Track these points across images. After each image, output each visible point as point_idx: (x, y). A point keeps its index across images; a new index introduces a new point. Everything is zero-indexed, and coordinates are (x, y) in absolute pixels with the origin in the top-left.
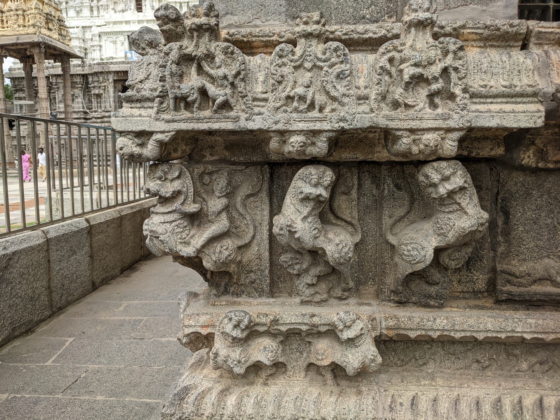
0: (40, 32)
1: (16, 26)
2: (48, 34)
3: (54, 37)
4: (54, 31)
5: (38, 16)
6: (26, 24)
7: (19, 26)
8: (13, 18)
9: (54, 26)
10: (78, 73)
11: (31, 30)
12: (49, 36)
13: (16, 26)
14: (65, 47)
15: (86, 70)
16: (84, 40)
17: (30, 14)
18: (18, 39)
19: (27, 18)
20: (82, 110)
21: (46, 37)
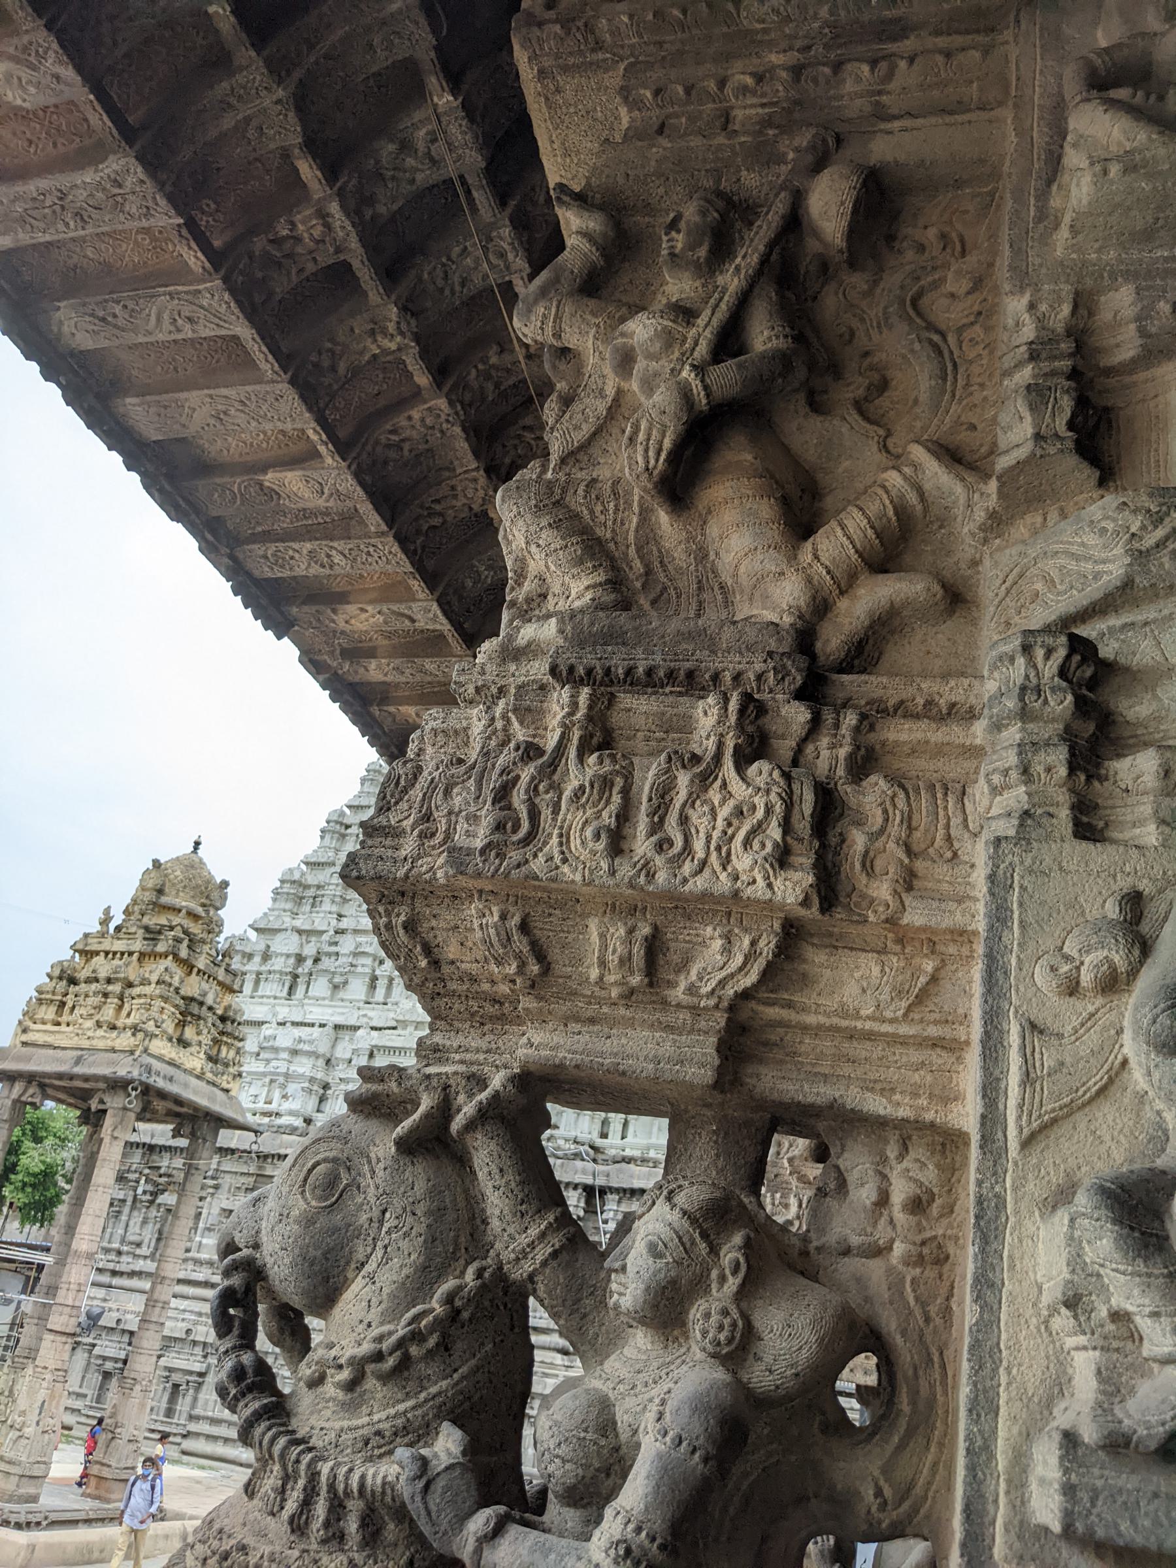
0: (146, 1050)
1: (89, 1024)
2: (173, 1055)
3: (188, 1066)
4: (194, 1049)
5: (158, 1003)
6: (119, 1024)
7: (99, 1025)
8: (90, 1001)
9: (198, 1034)
11: (125, 1040)
12: (171, 1063)
13: (89, 1024)
14: (212, 1099)
16: (328, 1062)
17: (139, 996)
18: (78, 1060)
19: (127, 1006)
21: (157, 1065)
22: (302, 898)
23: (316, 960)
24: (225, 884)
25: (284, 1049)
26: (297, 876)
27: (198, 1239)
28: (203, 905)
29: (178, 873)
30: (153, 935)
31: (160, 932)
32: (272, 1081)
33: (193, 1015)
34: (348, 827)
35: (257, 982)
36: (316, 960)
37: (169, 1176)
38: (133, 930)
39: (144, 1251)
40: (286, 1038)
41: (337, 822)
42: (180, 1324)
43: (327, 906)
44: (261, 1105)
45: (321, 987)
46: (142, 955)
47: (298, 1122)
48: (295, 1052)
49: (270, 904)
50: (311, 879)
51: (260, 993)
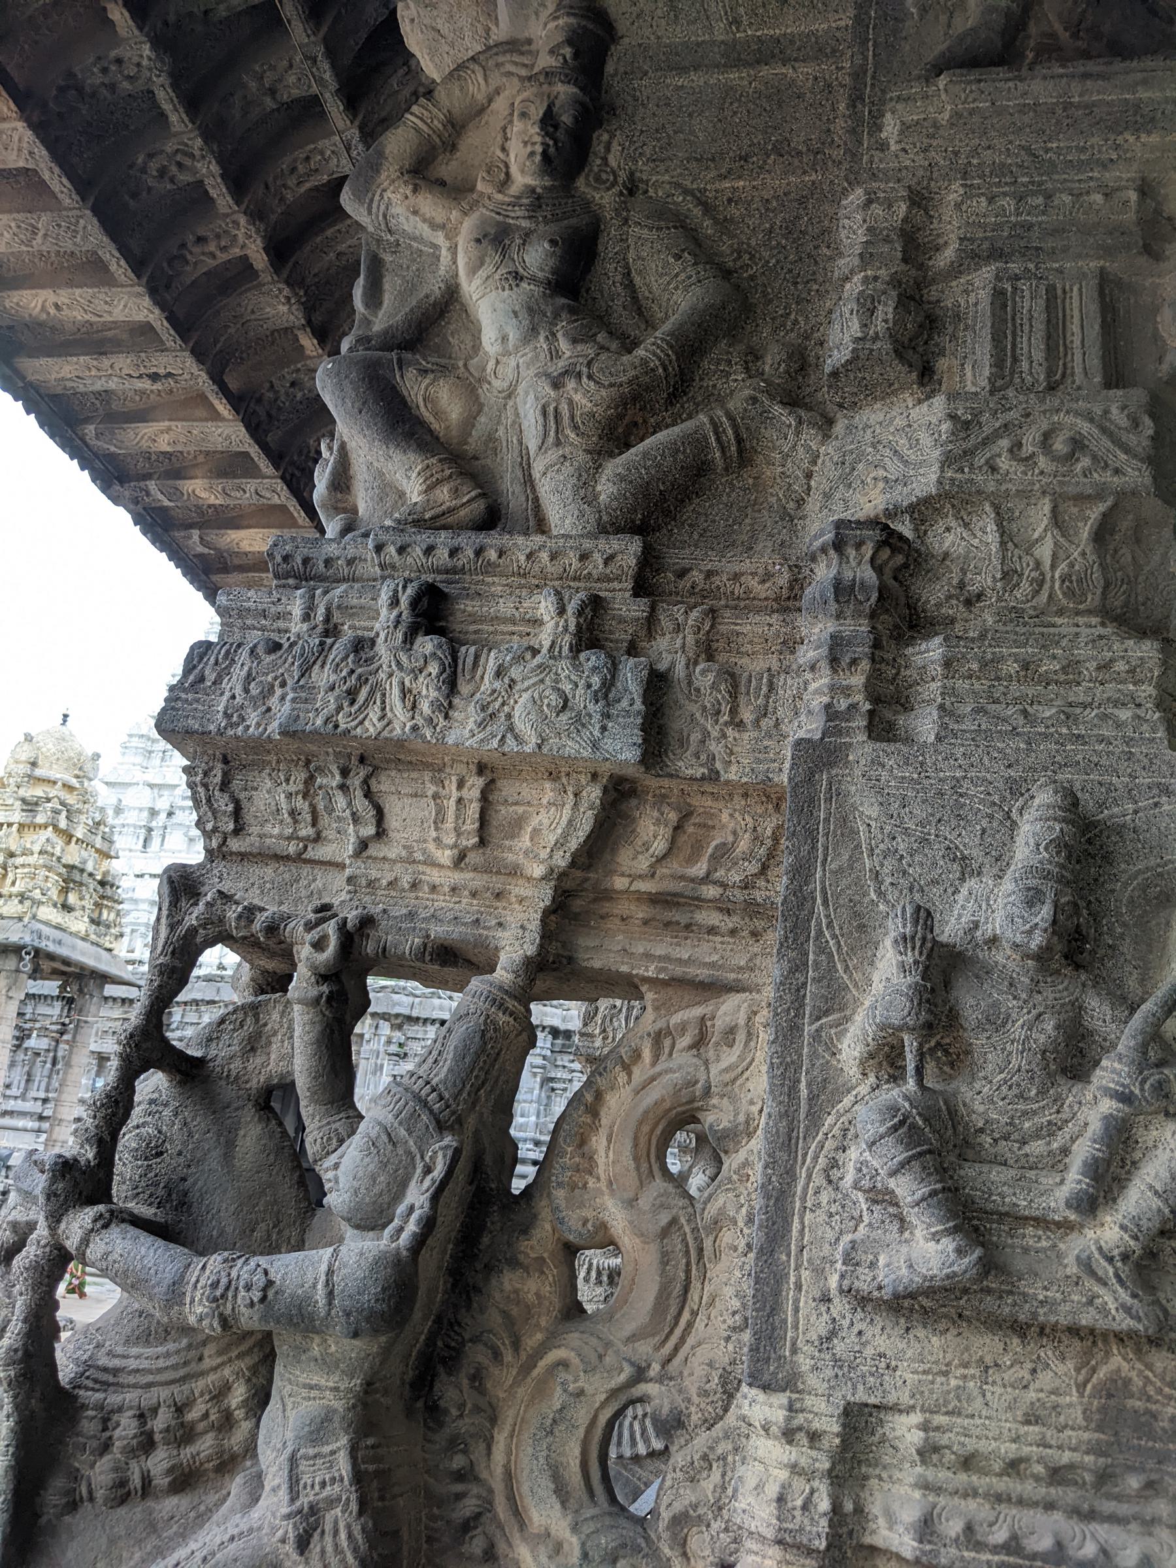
0: (34, 917)
2: (59, 920)
3: (73, 929)
4: (78, 913)
5: (43, 872)
9: (81, 899)
14: (98, 959)
17: (23, 866)
19: (11, 876)
22: (150, 752)
23: (170, 814)
24: (96, 757)
25: (143, 901)
28: (77, 777)
29: (50, 746)
30: (31, 806)
31: (36, 804)
33: (75, 882)
36: (170, 814)
38: (10, 802)
39: (14, 1091)
46: (22, 826)
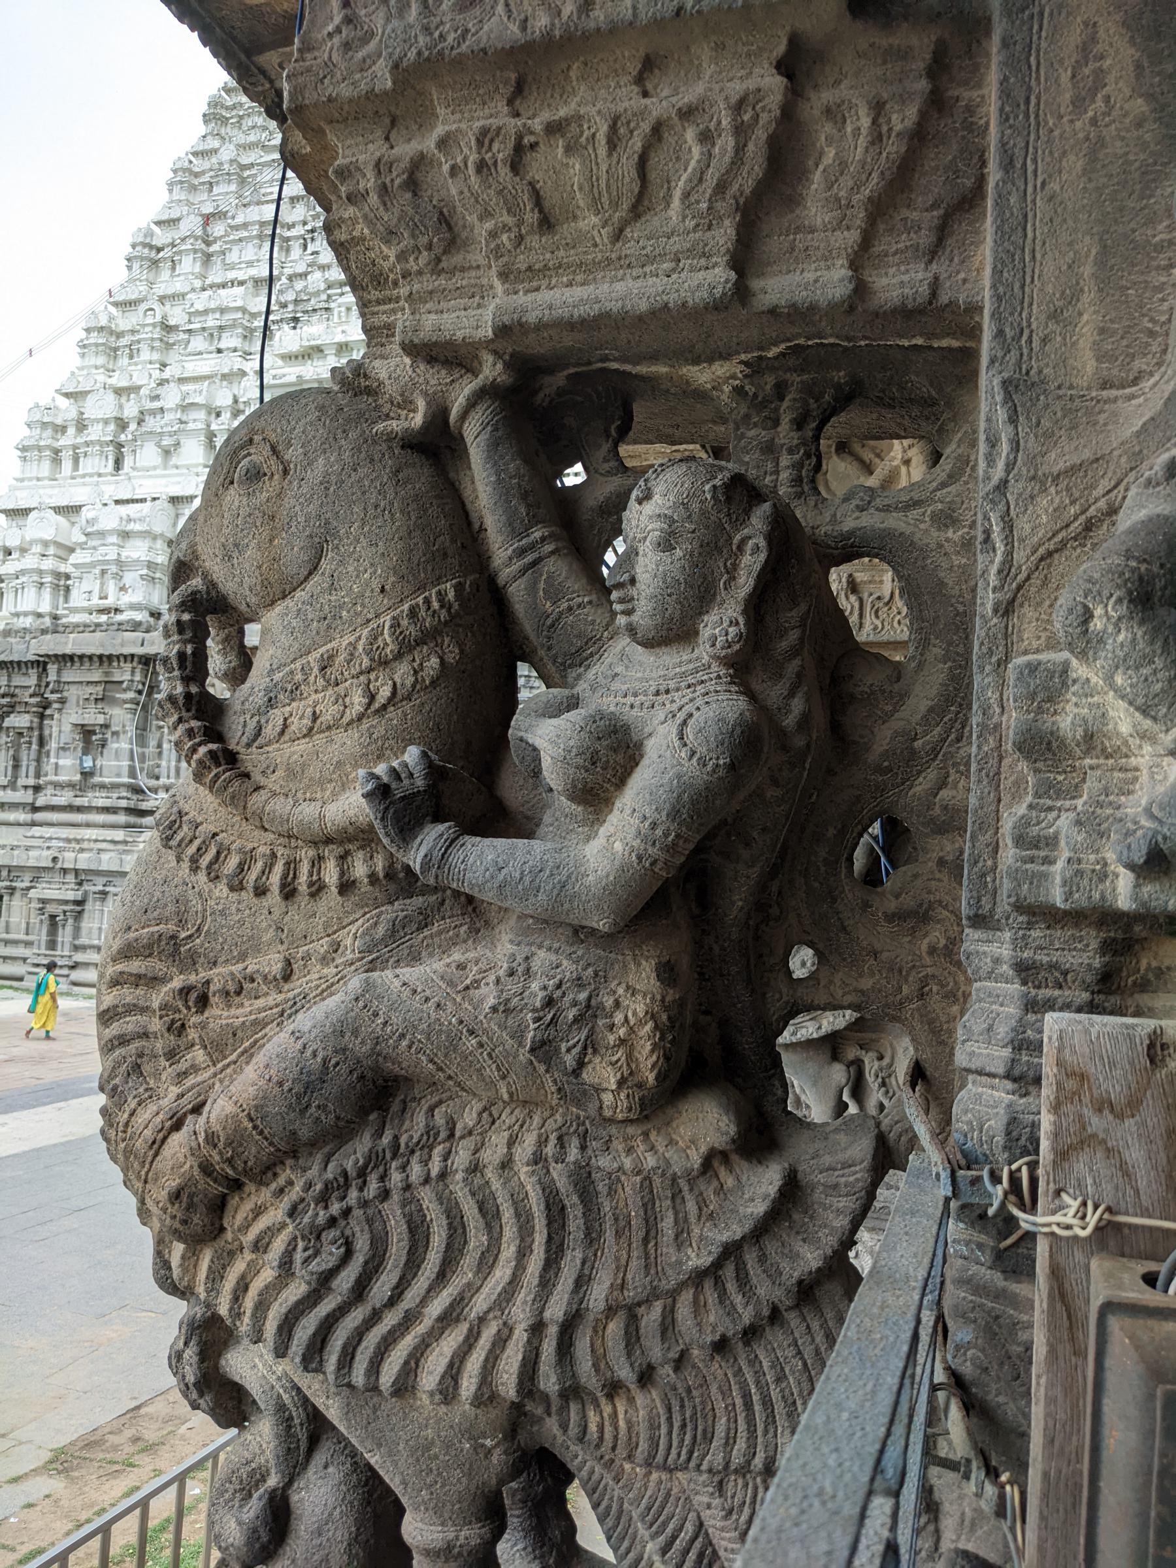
10: (127, 651)
15: (153, 643)
20: (126, 780)
22: (116, 349)
23: (140, 422)
25: (111, 532)
26: (103, 322)
27: (53, 760)
32: (103, 572)
34: (159, 250)
35: (76, 460)
36: (140, 422)
37: (13, 696)
40: (110, 519)
41: (145, 245)
42: (46, 853)
43: (146, 355)
44: (96, 601)
45: (149, 454)
47: (139, 616)
48: (126, 535)
49: (78, 362)
50: (124, 322)
51: (81, 472)
